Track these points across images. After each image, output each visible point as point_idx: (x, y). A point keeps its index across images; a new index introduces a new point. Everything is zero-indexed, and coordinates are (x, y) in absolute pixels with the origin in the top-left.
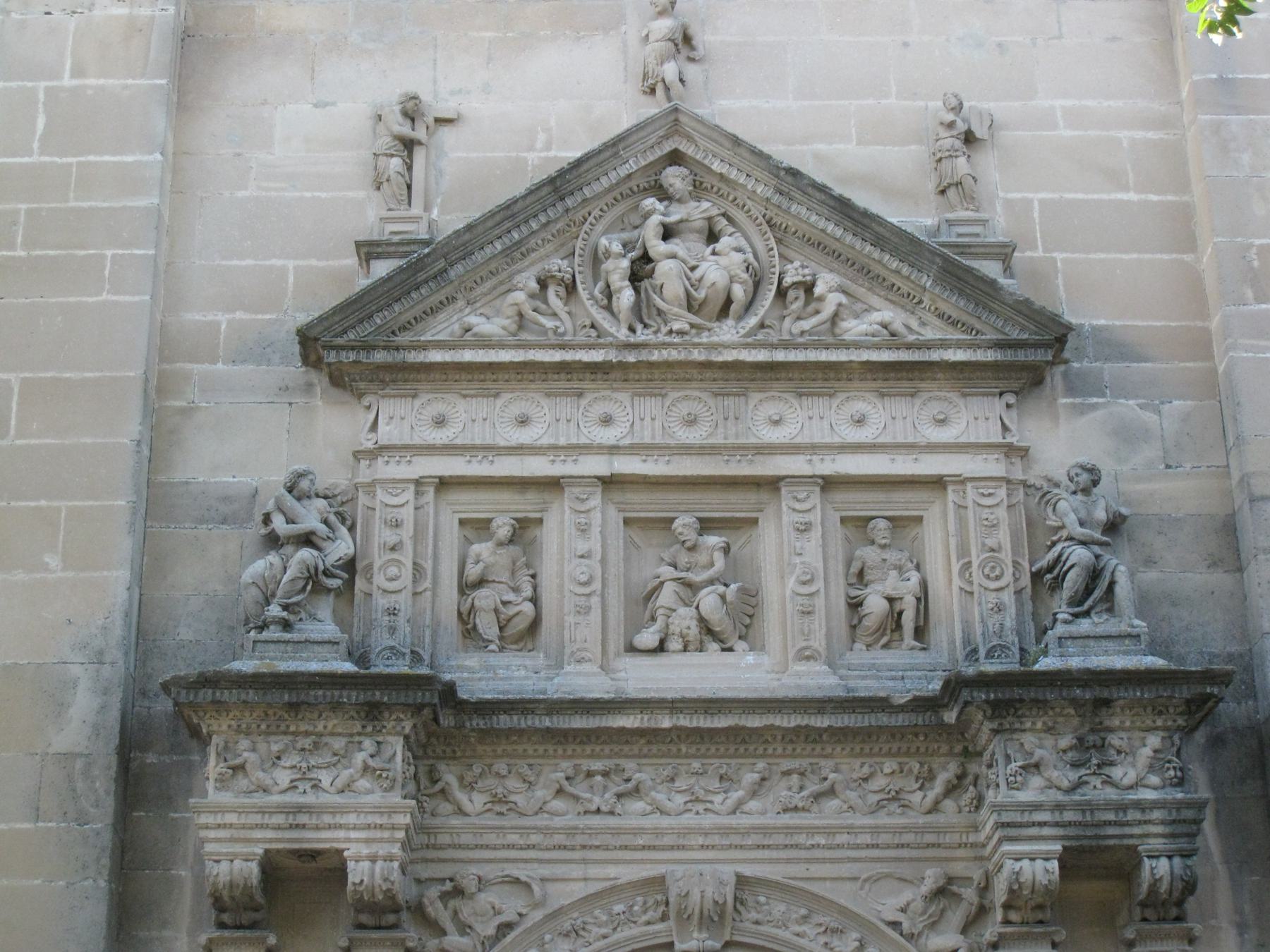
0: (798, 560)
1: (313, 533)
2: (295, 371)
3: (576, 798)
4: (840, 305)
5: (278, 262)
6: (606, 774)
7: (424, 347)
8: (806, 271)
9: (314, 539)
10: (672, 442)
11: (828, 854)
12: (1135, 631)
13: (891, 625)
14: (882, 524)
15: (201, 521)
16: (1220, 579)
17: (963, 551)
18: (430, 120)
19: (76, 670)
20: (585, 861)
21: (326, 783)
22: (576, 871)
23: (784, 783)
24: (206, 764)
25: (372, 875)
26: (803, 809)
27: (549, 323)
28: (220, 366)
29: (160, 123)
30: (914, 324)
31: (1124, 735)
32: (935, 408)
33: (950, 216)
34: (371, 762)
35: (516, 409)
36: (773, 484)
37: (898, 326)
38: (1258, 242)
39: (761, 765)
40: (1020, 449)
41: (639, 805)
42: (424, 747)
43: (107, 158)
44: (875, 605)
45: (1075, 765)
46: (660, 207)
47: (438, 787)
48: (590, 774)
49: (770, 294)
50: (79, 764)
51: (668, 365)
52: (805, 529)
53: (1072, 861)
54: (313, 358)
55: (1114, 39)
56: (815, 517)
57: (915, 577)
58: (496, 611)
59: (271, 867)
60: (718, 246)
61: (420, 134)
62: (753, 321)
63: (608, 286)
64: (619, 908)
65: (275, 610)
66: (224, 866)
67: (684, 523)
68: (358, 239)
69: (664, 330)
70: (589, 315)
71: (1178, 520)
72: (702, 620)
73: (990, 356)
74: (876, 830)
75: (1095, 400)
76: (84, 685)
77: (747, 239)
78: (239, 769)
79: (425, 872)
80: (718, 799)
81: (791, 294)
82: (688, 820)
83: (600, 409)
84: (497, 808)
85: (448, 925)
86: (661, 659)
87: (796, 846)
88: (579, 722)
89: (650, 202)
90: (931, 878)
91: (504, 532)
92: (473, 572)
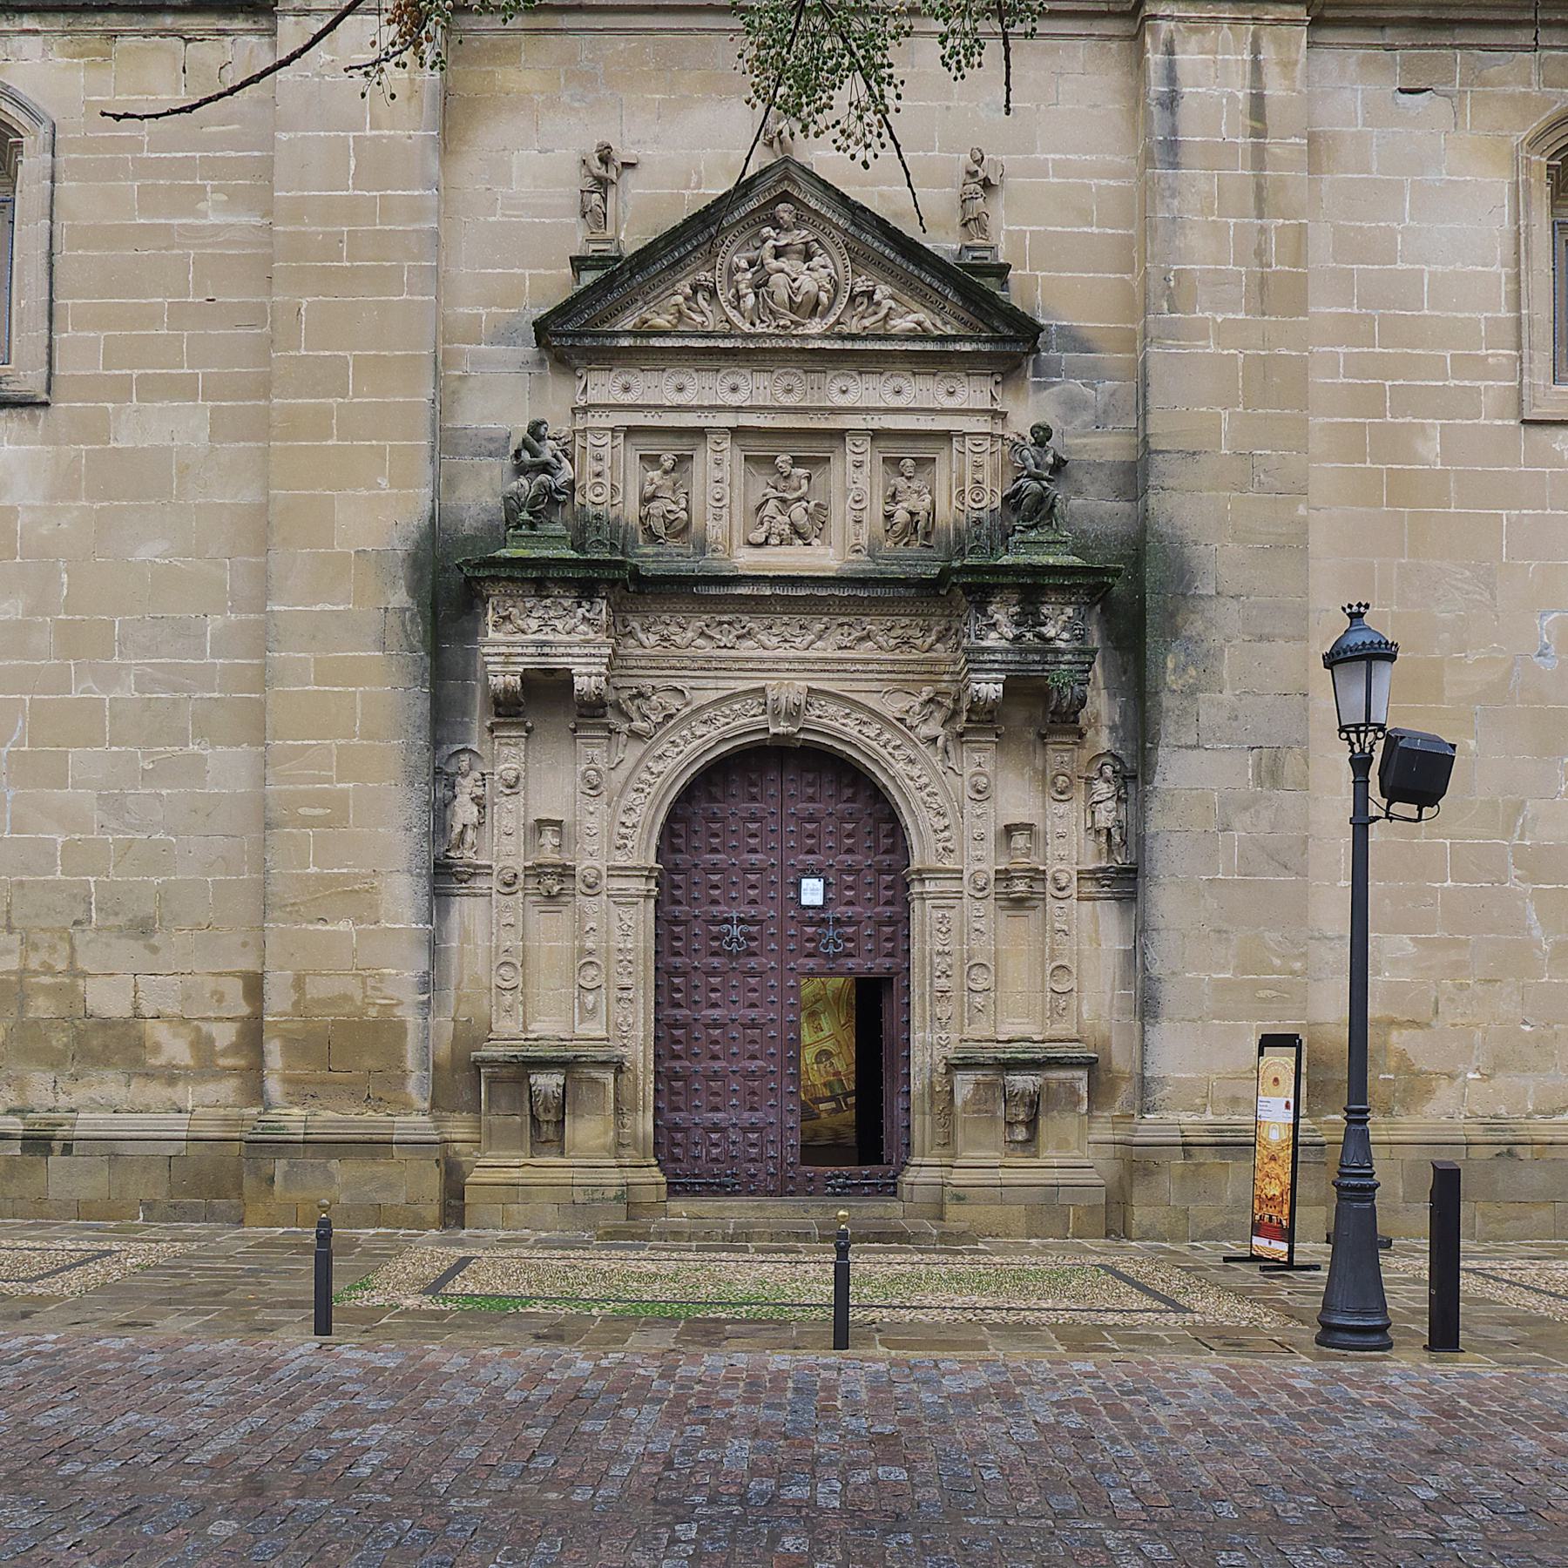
0: (854, 486)
1: (548, 463)
2: (530, 350)
3: (712, 638)
4: (890, 308)
6: (730, 623)
7: (616, 335)
8: (870, 283)
10: (777, 404)
11: (864, 676)
13: (910, 530)
14: (909, 462)
16: (1123, 506)
17: (961, 482)
18: (618, 164)
20: (716, 678)
21: (560, 627)
22: (711, 684)
23: (839, 631)
24: (486, 615)
25: (589, 685)
26: (850, 648)
27: (699, 319)
28: (483, 346)
29: (434, 165)
30: (939, 324)
31: (1050, 607)
32: (947, 384)
33: (969, 243)
34: (587, 614)
35: (676, 380)
36: (840, 434)
37: (928, 324)
38: (1175, 267)
39: (825, 619)
40: (1001, 413)
41: (751, 643)
42: (619, 604)
44: (901, 516)
45: (1018, 625)
46: (773, 234)
47: (629, 629)
48: (721, 623)
49: (844, 299)
51: (774, 351)
52: (858, 466)
53: (1012, 687)
54: (544, 341)
55: (1095, 106)
56: (867, 458)
57: (928, 498)
58: (663, 516)
59: (526, 677)
60: (812, 264)
61: (613, 175)
62: (832, 319)
63: (738, 291)
64: (736, 707)
65: (525, 515)
66: (500, 679)
67: (783, 459)
69: (774, 324)
70: (725, 313)
72: (792, 524)
73: (986, 348)
74: (893, 662)
77: (832, 259)
78: (507, 618)
79: (620, 683)
80: (799, 640)
81: (859, 300)
82: (780, 653)
83: (730, 381)
84: (665, 644)
85: (635, 715)
86: (767, 550)
87: (845, 671)
88: (713, 591)
89: (767, 231)
90: (927, 692)
91: (668, 464)
92: (649, 490)
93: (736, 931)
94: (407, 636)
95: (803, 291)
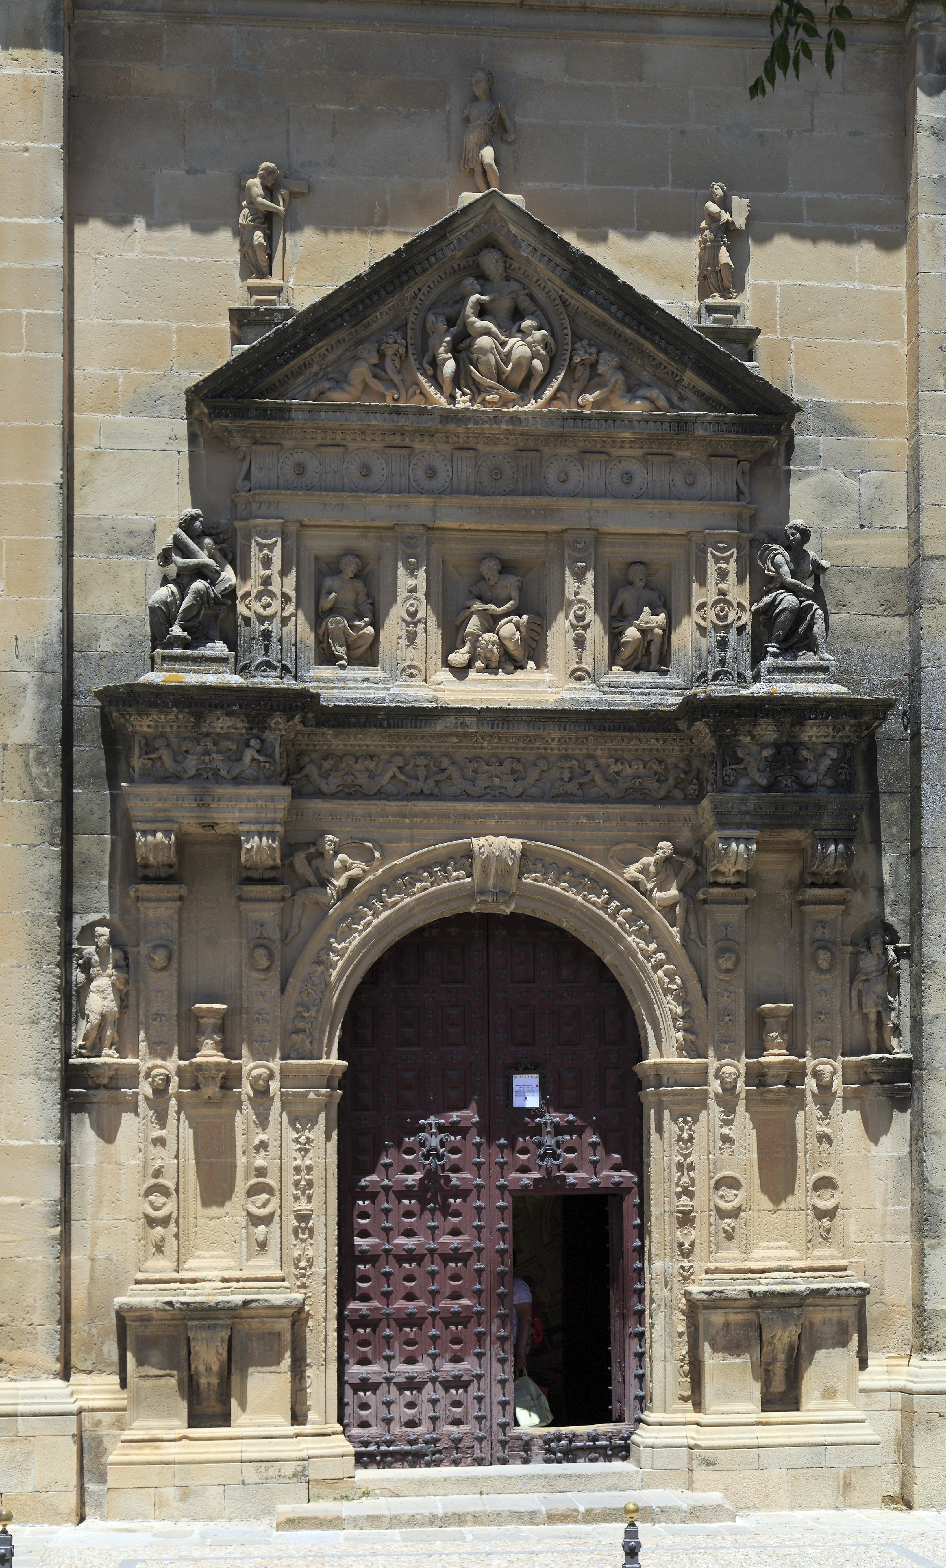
5: (164, 323)
9: (205, 571)
12: (826, 663)
15: (112, 552)
19: (25, 678)
43: (15, 220)
50: (32, 753)
68: (232, 307)
71: (864, 571)
75: (811, 468)
76: (31, 689)
93: (434, 1142)
94: (32, 779)
95: (515, 356)
